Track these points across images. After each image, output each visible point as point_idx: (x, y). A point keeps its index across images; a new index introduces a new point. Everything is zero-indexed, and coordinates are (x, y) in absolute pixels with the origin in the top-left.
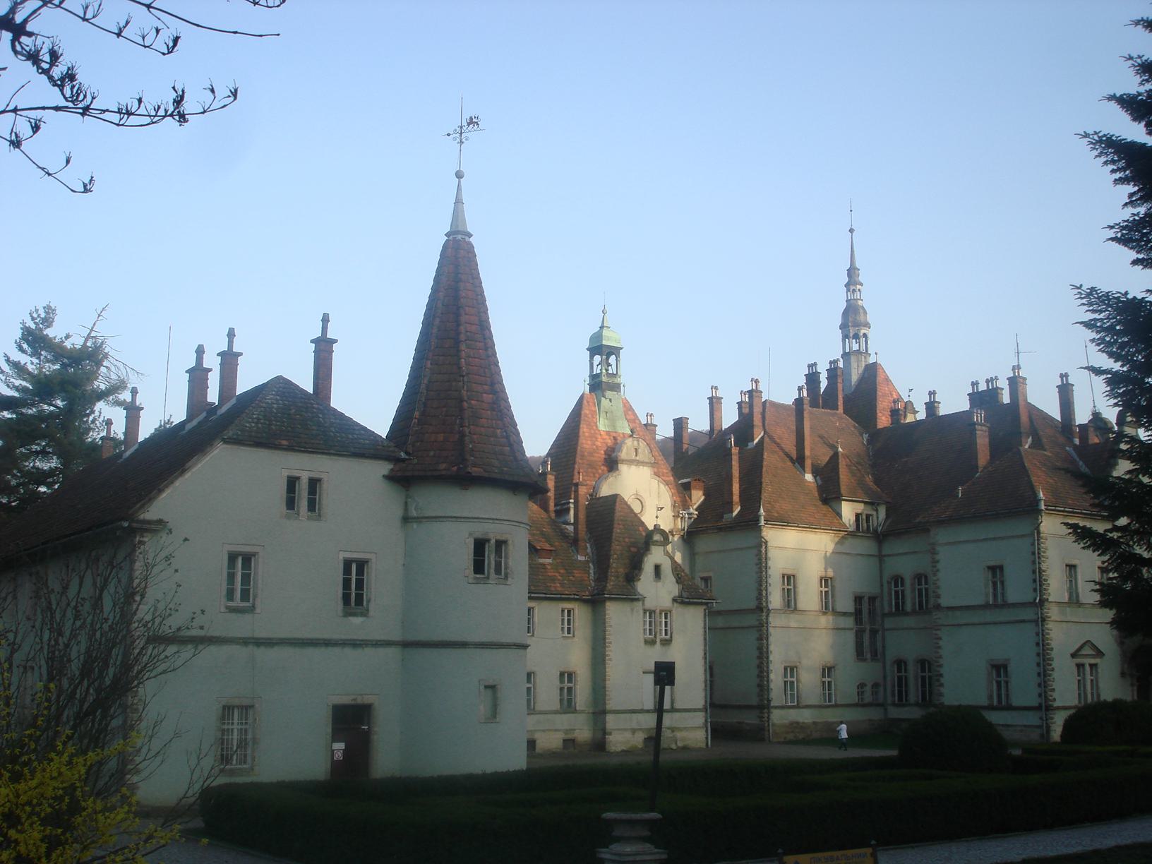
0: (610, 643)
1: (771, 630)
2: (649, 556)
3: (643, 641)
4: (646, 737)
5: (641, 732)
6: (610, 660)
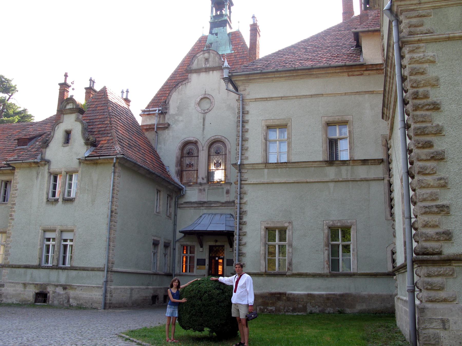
0: (14, 204)
1: (246, 188)
2: (61, 124)
3: (45, 200)
4: (37, 291)
5: (32, 286)
6: (13, 219)
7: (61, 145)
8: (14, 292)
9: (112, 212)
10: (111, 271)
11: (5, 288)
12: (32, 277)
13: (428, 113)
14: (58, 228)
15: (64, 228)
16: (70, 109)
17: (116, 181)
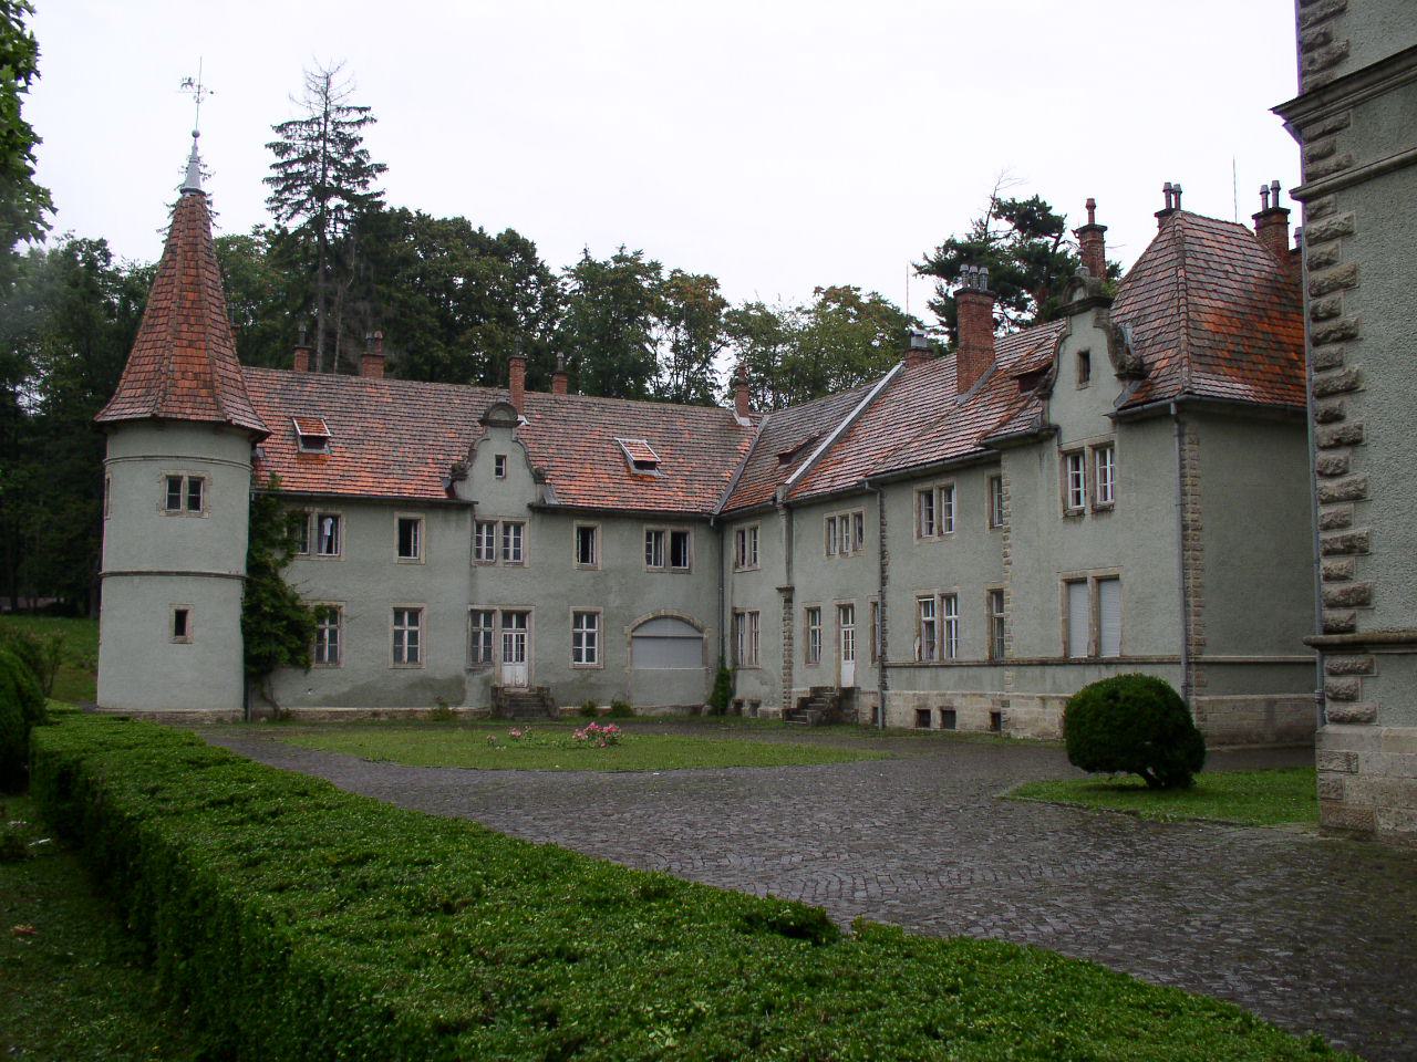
0: (1008, 531)
3: (1061, 516)
7: (1074, 387)
8: (1027, 717)
9: (1185, 528)
10: (1197, 664)
11: (1011, 708)
12: (1054, 682)
13: (1333, 349)
14: (1090, 574)
15: (1101, 573)
16: (1079, 302)
17: (1187, 455)
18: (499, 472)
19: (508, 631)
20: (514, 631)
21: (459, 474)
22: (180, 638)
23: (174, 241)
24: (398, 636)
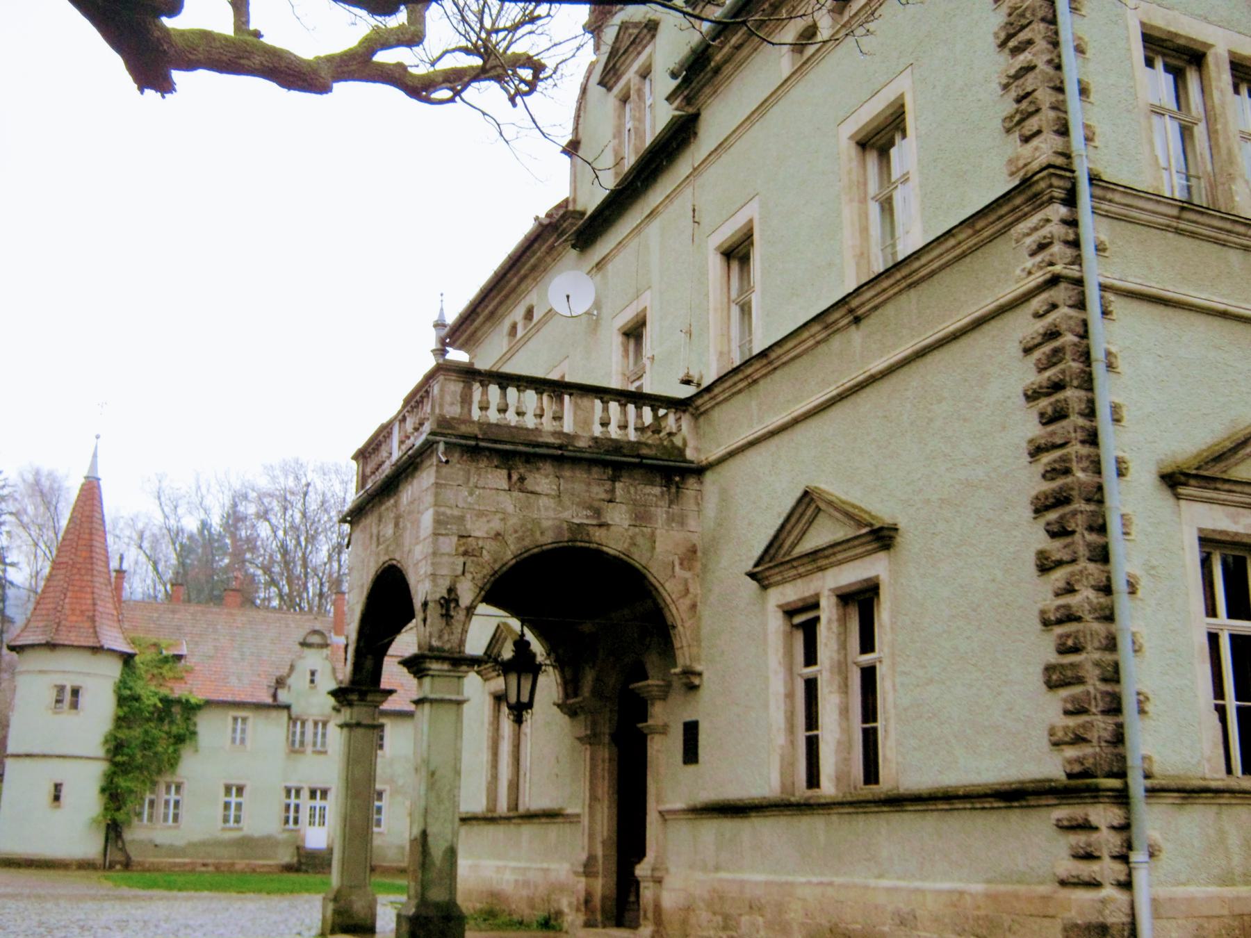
18: (312, 681)
19: (313, 803)
20: (318, 803)
21: (280, 683)
22: (56, 804)
23: (75, 514)
24: (227, 806)
